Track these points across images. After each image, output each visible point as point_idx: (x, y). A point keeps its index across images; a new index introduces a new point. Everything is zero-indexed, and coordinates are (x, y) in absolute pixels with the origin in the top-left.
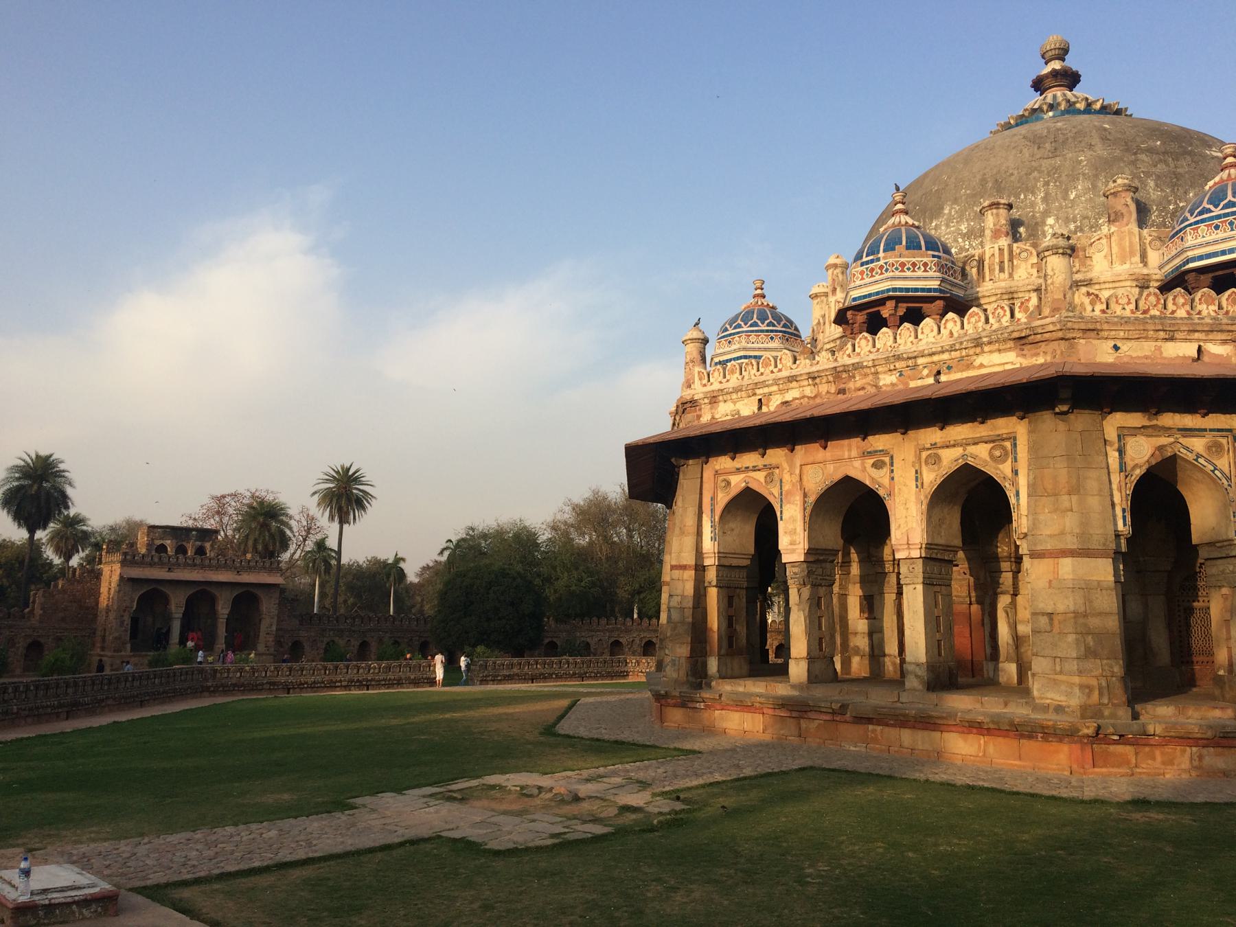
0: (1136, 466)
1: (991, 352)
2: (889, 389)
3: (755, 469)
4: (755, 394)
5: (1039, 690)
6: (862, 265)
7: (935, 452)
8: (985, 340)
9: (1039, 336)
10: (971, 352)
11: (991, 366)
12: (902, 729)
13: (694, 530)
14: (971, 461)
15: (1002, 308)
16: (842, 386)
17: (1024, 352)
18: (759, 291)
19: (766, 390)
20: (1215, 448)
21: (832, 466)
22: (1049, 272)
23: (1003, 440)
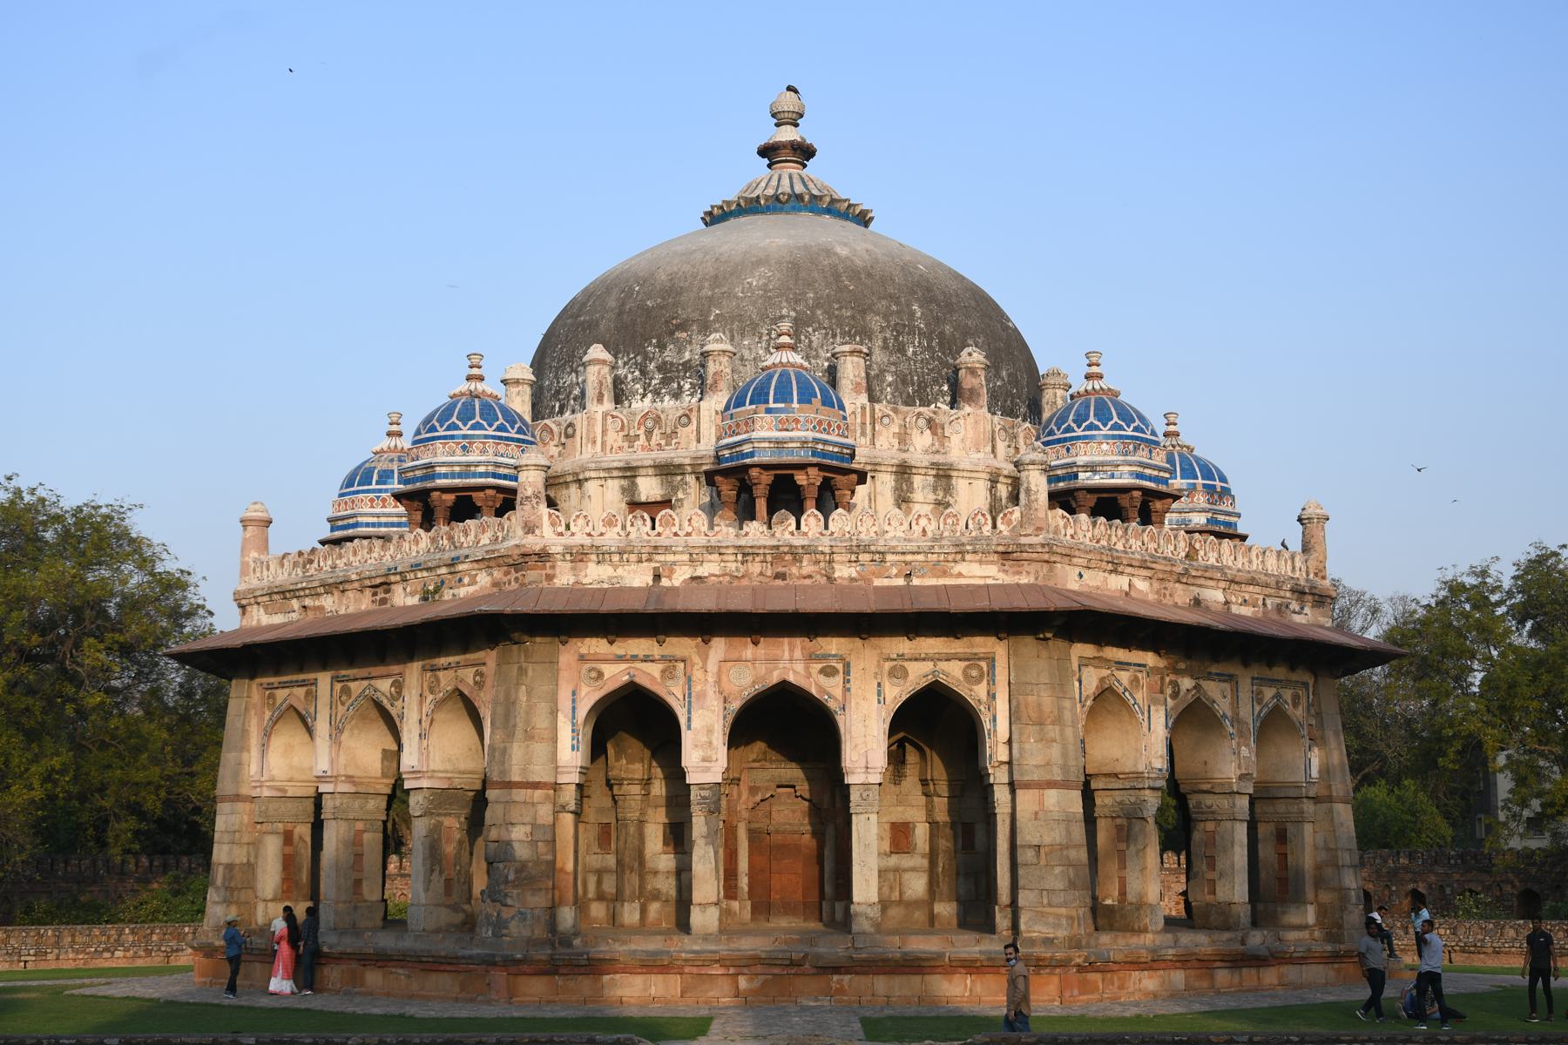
0: (1088, 697)
1: (971, 561)
2: (845, 583)
3: (647, 659)
4: (649, 560)
5: (1026, 924)
6: (769, 411)
7: (900, 663)
8: (969, 548)
9: (1025, 555)
10: (950, 558)
11: (971, 577)
12: (876, 977)
13: (546, 734)
14: (942, 679)
15: (983, 515)
16: (780, 569)
17: (1006, 568)
18: (475, 371)
19: (670, 558)
20: (1135, 681)
21: (763, 666)
22: (1033, 488)
23: (979, 659)
